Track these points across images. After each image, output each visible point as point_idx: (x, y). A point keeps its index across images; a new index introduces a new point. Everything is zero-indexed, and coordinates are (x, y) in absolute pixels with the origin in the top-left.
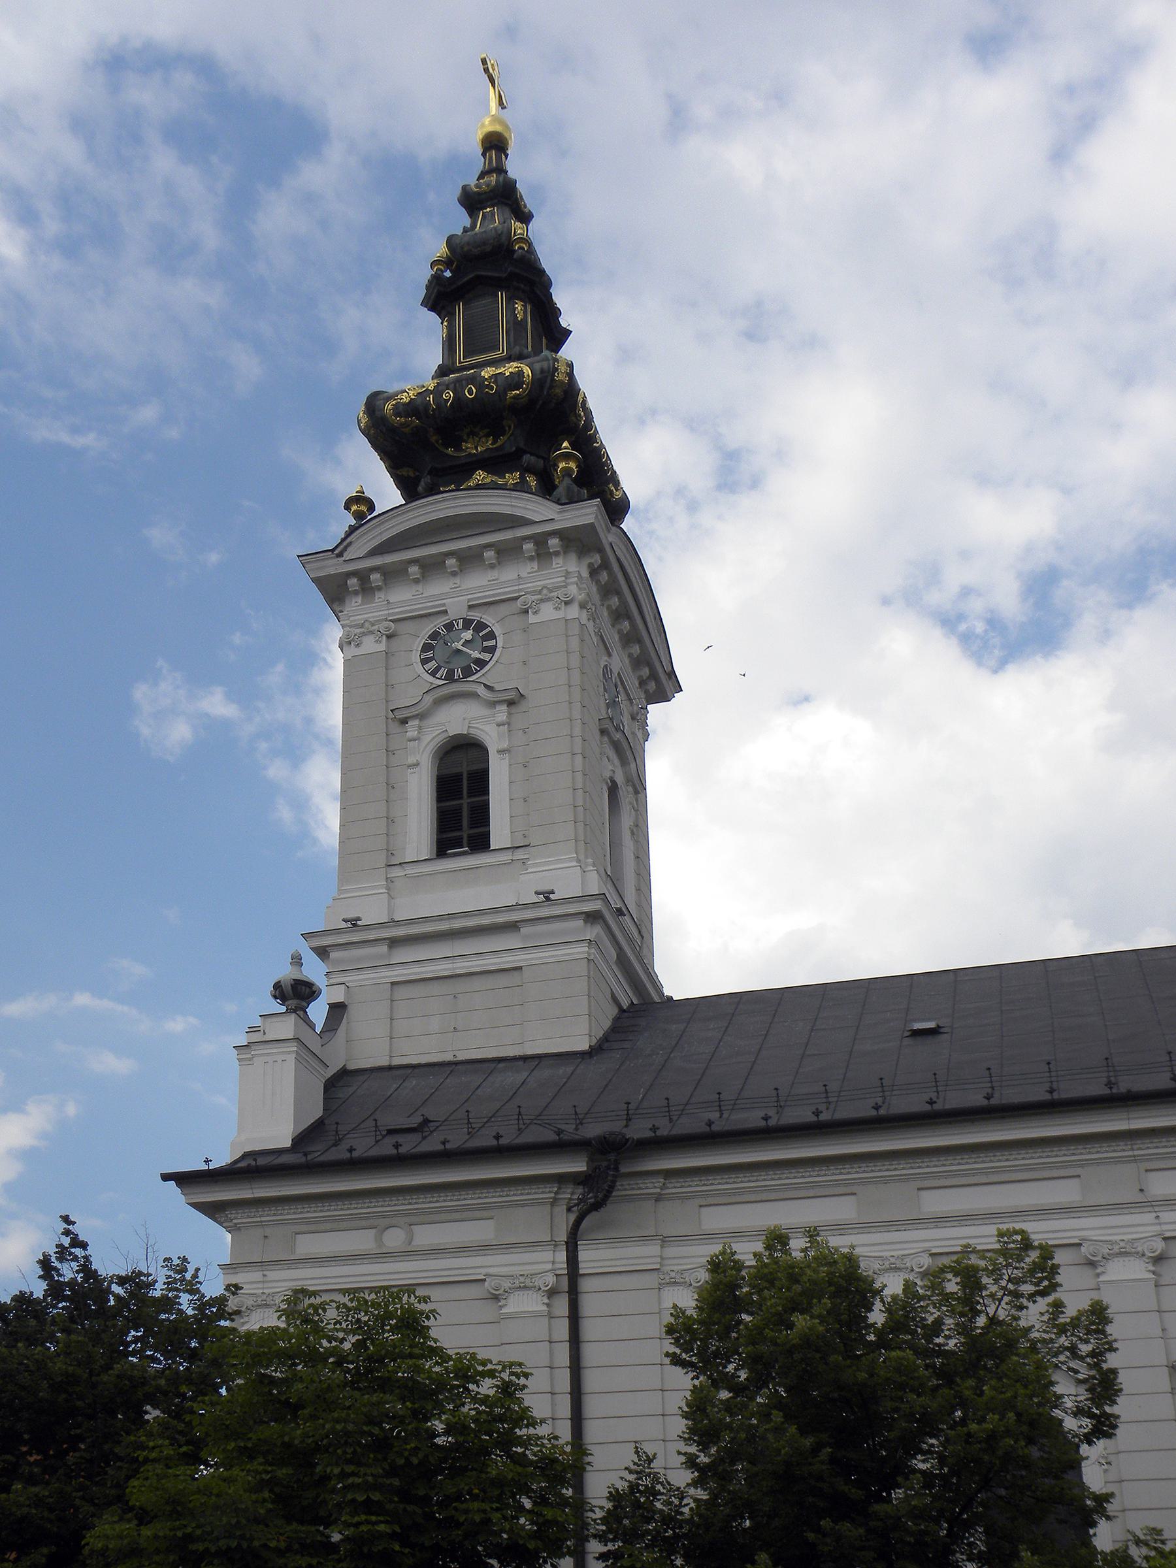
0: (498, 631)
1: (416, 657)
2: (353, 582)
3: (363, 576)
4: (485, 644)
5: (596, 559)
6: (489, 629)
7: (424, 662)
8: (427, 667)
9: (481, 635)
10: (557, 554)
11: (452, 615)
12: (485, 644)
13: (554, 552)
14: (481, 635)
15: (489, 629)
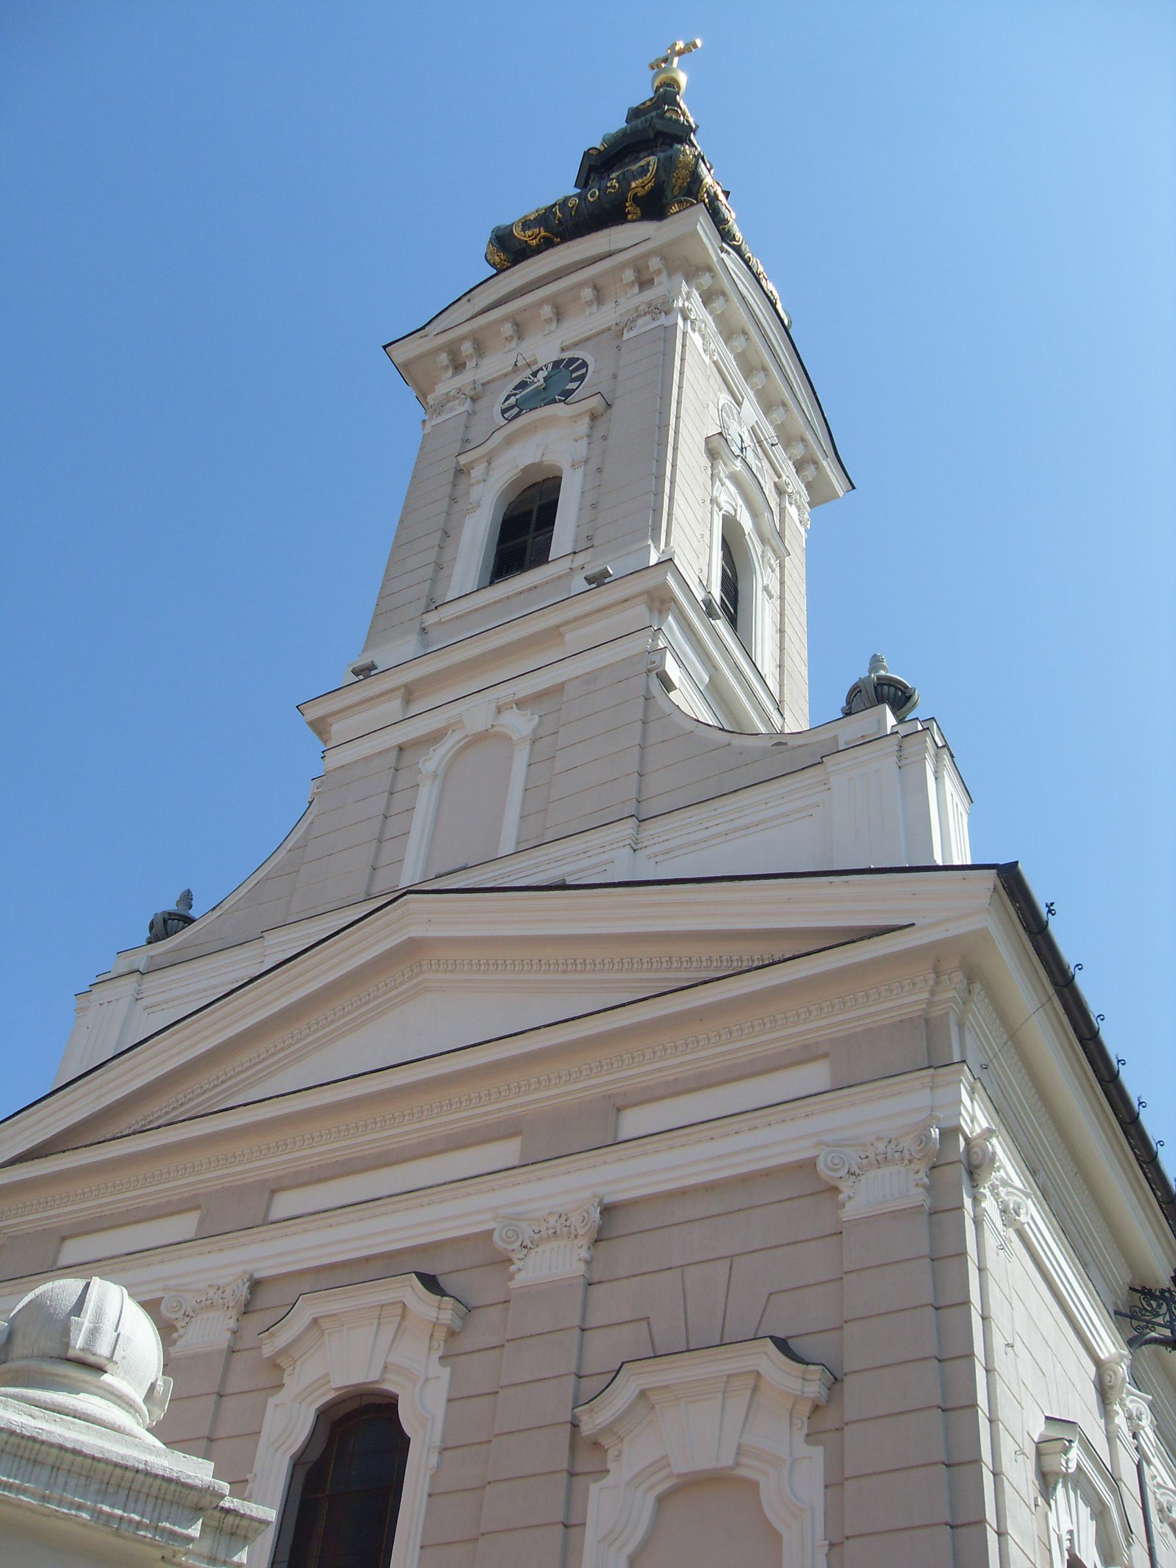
0: (589, 359)
1: (497, 409)
2: (444, 358)
3: (453, 351)
4: (574, 375)
5: (706, 280)
6: (581, 361)
7: (504, 412)
8: (506, 415)
9: (570, 369)
10: (659, 272)
11: (541, 364)
12: (574, 375)
13: (655, 272)
14: (570, 369)
15: (581, 361)
